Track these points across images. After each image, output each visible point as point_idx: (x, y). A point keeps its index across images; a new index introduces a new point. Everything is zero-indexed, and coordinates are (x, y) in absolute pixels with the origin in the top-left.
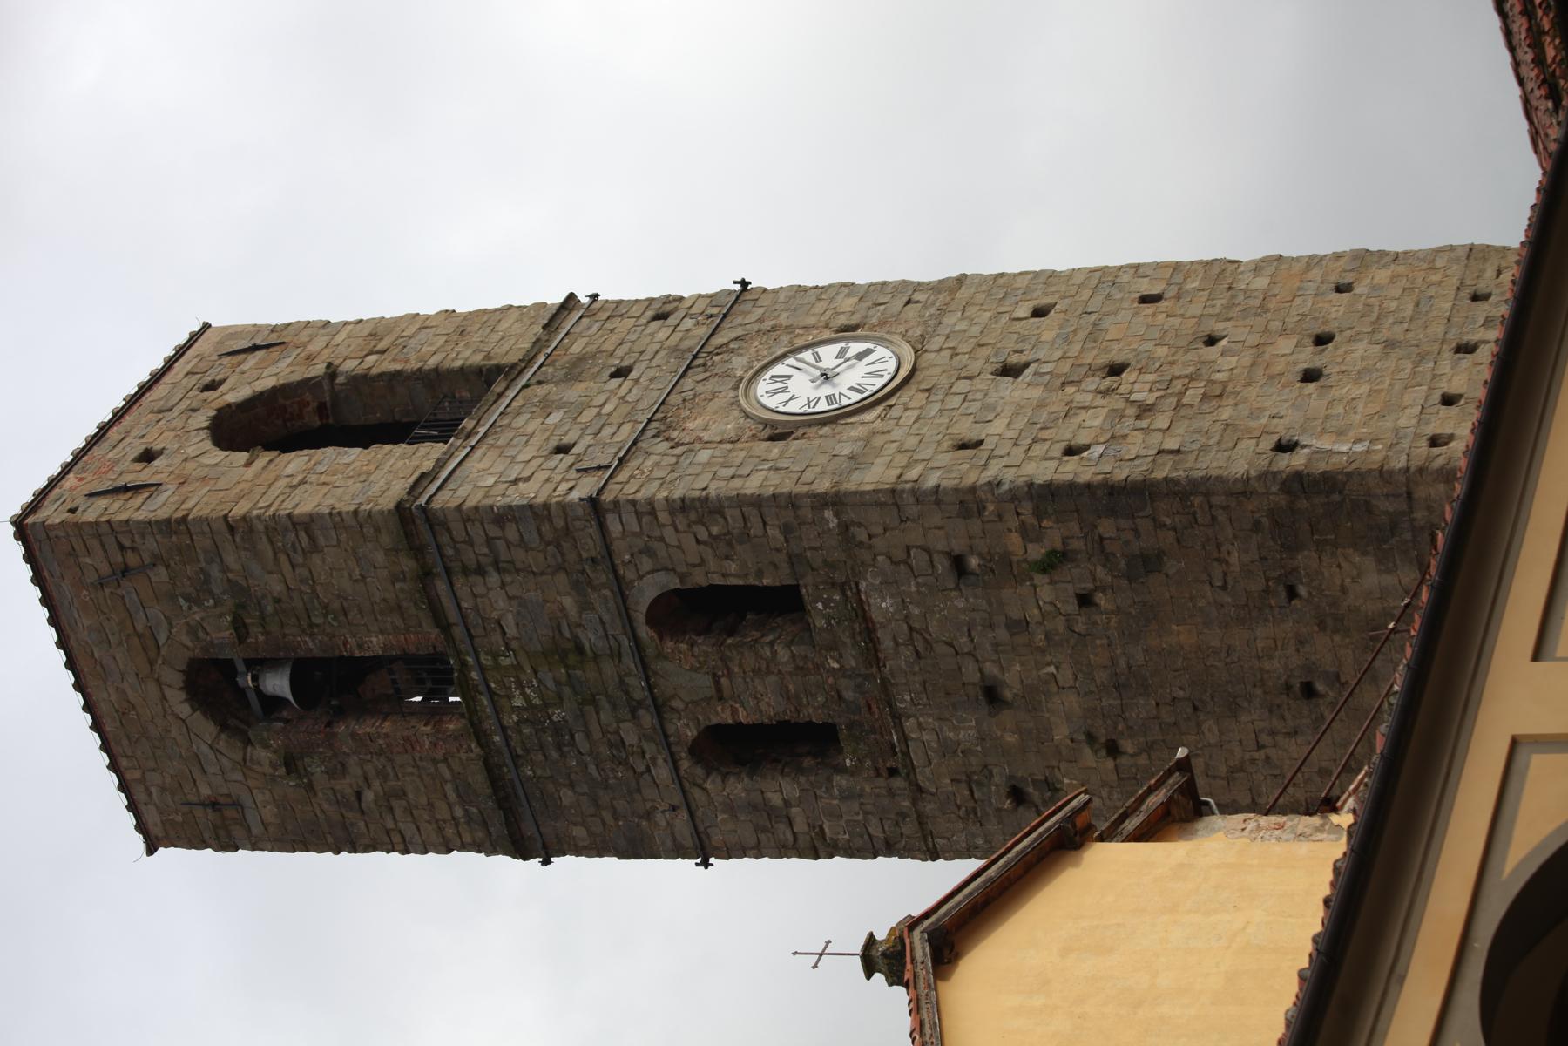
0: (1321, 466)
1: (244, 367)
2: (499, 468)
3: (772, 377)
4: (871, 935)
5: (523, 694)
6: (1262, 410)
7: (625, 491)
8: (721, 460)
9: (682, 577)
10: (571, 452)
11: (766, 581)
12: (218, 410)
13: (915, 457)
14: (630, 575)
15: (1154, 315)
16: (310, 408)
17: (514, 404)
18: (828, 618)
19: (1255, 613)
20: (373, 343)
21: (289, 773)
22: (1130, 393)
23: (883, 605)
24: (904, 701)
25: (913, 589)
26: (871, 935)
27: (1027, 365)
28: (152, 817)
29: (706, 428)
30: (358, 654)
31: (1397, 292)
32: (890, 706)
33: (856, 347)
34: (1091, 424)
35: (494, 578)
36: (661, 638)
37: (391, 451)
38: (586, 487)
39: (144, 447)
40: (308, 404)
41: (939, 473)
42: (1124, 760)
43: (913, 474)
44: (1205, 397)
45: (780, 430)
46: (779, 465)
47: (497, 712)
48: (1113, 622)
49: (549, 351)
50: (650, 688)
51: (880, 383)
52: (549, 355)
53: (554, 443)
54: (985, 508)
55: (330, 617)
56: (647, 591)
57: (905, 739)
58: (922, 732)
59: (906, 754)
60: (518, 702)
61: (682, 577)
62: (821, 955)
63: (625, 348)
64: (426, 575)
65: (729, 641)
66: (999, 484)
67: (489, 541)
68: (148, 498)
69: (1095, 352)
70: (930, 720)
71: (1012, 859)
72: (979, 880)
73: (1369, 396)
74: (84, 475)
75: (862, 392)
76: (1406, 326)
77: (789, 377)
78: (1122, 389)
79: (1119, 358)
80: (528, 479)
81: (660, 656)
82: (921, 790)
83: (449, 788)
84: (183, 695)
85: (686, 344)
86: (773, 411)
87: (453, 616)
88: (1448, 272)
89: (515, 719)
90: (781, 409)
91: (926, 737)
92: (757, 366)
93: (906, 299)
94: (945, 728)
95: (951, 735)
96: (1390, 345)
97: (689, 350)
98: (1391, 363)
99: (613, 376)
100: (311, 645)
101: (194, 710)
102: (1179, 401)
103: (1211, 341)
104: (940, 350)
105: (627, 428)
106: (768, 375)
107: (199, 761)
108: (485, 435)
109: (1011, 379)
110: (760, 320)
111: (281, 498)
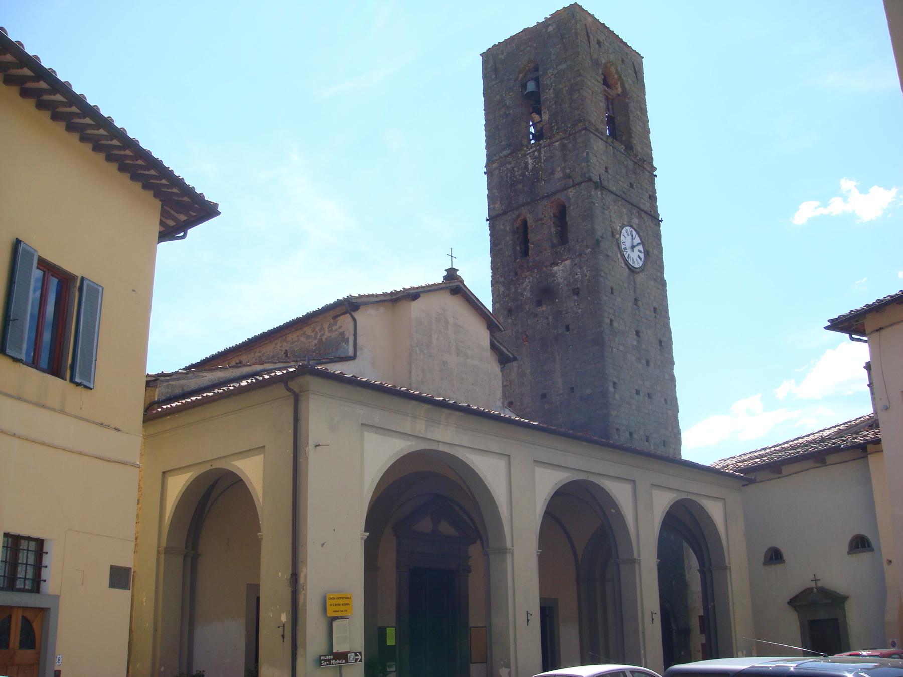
4: (458, 270)
26: (458, 270)
33: (642, 256)
51: (631, 263)
90: (622, 234)
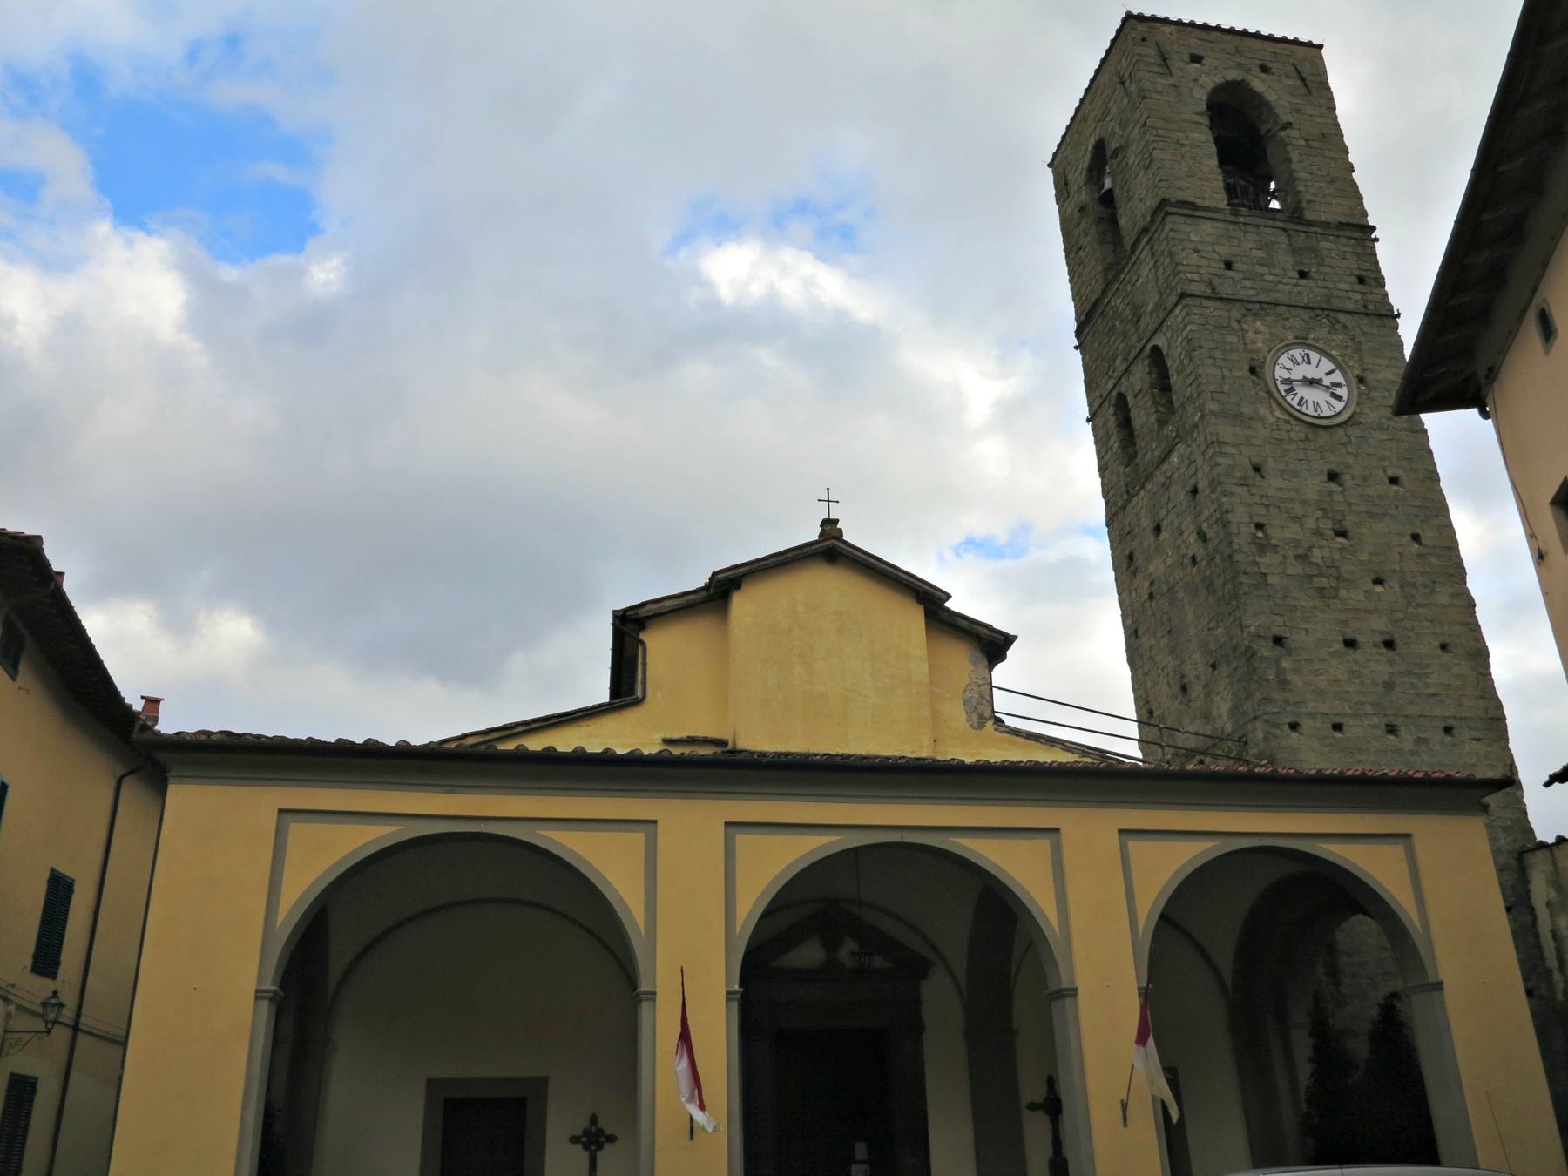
4: (838, 521)
9: (1167, 355)
14: (1164, 329)
17: (1267, 230)
19: (1203, 649)
24: (1149, 486)
26: (838, 521)
32: (1146, 480)
42: (1148, 604)
56: (1159, 341)
61: (1167, 355)
62: (828, 501)
68: (1159, 73)
71: (892, 573)
72: (874, 561)
81: (1143, 360)
82: (1125, 509)
83: (1089, 288)
87: (1137, 253)
91: (1140, 503)
105: (1251, 292)
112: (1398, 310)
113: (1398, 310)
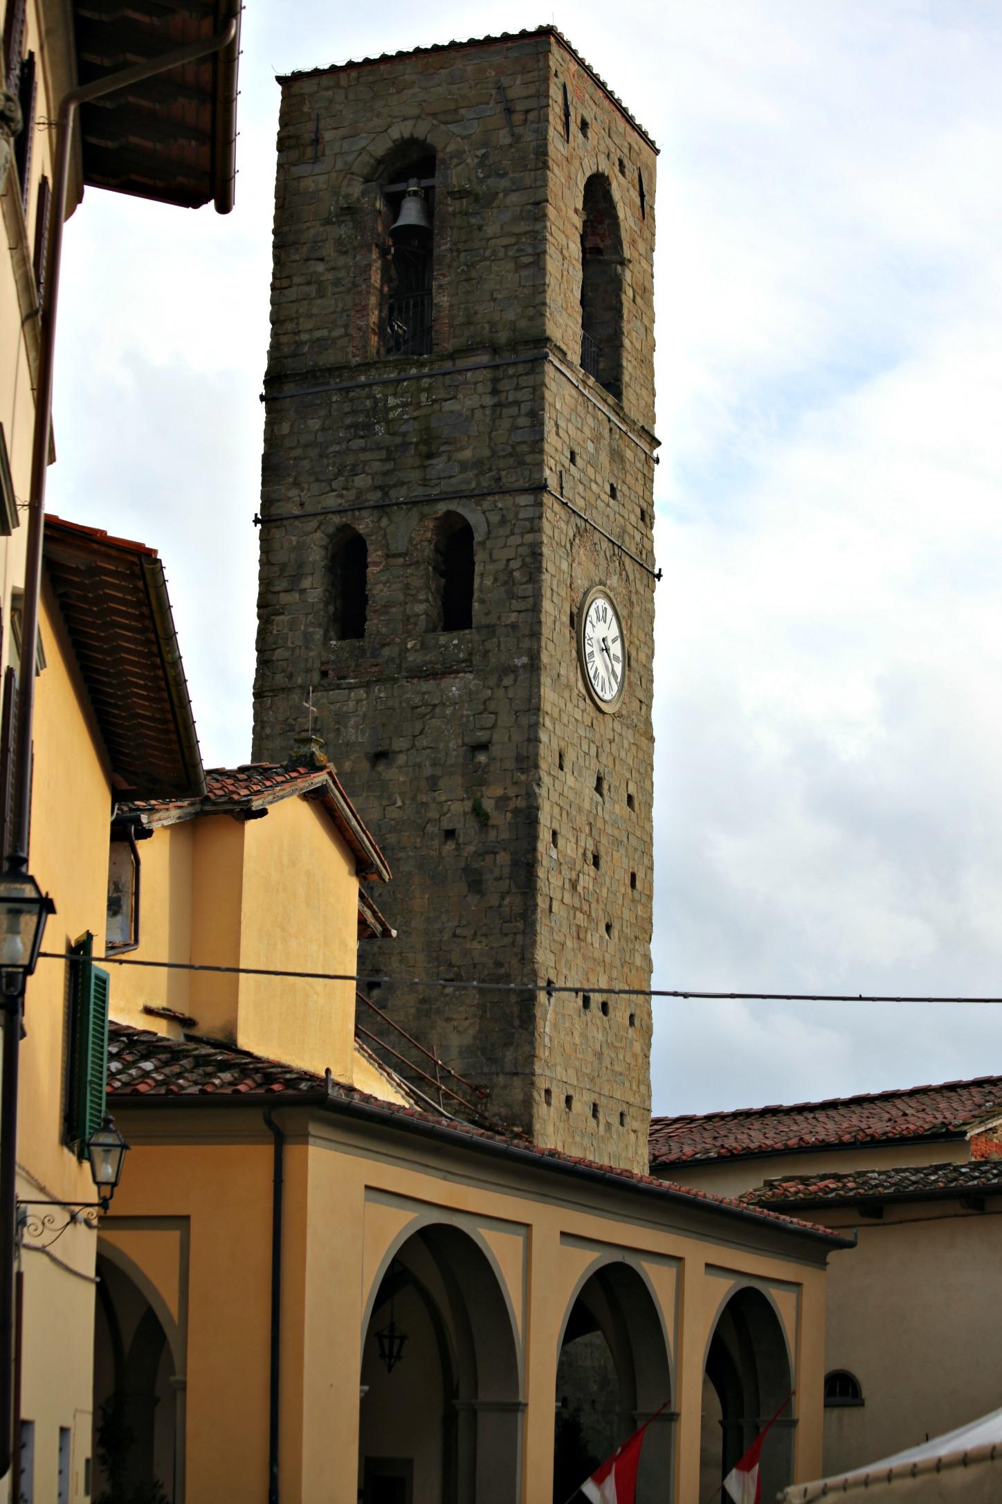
0: (538, 1013)
1: (632, 190)
2: (565, 412)
3: (606, 609)
5: (397, 406)
6: (570, 969)
7: (548, 510)
8: (562, 579)
10: (571, 465)
11: (476, 605)
12: (608, 177)
13: (557, 722)
14: (486, 504)
15: (625, 884)
16: (599, 241)
17: (600, 413)
18: (446, 647)
19: (434, 955)
20: (640, 292)
21: (342, 209)
22: (584, 873)
23: (454, 689)
24: (380, 692)
25: (465, 713)
27: (601, 795)
28: (308, 87)
29: (579, 563)
30: (434, 283)
31: (628, 1059)
32: (376, 681)
33: (618, 668)
34: (568, 847)
35: (489, 401)
36: (435, 519)
37: (578, 323)
38: (552, 482)
39: (590, 122)
40: (603, 241)
41: (547, 741)
43: (548, 723)
44: (579, 927)
45: (577, 621)
46: (557, 623)
47: (384, 383)
48: (432, 853)
49: (629, 433)
50: (398, 504)
51: (598, 689)
52: (626, 434)
53: (577, 450)
54: (523, 773)
55: (465, 269)
56: (474, 516)
57: (351, 688)
58: (355, 701)
59: (339, 687)
60: (391, 401)
61: (483, 543)
63: (627, 492)
64: (495, 350)
65: (430, 568)
66: (539, 785)
67: (517, 403)
69: (607, 845)
70: (364, 709)
73: (574, 1044)
74: (576, 77)
75: (594, 678)
76: (609, 1067)
77: (605, 622)
78: (585, 866)
79: (602, 863)
80: (557, 434)
81: (423, 517)
83: (325, 333)
84: (407, 135)
85: (627, 538)
86: (587, 613)
87: (461, 363)
88: (637, 1095)
89: (378, 396)
90: (589, 619)
92: (611, 595)
93: (643, 700)
94: (357, 719)
95: (352, 722)
96: (599, 1055)
97: (623, 542)
98: (590, 1058)
99: (612, 485)
100: (443, 248)
101: (394, 141)
102: (577, 909)
103: (608, 928)
104: (613, 730)
106: (607, 606)
107: (352, 137)
108: (583, 395)
109: (595, 786)
110: (637, 592)
111: (556, 244)
112: (660, 570)
113: (660, 570)
